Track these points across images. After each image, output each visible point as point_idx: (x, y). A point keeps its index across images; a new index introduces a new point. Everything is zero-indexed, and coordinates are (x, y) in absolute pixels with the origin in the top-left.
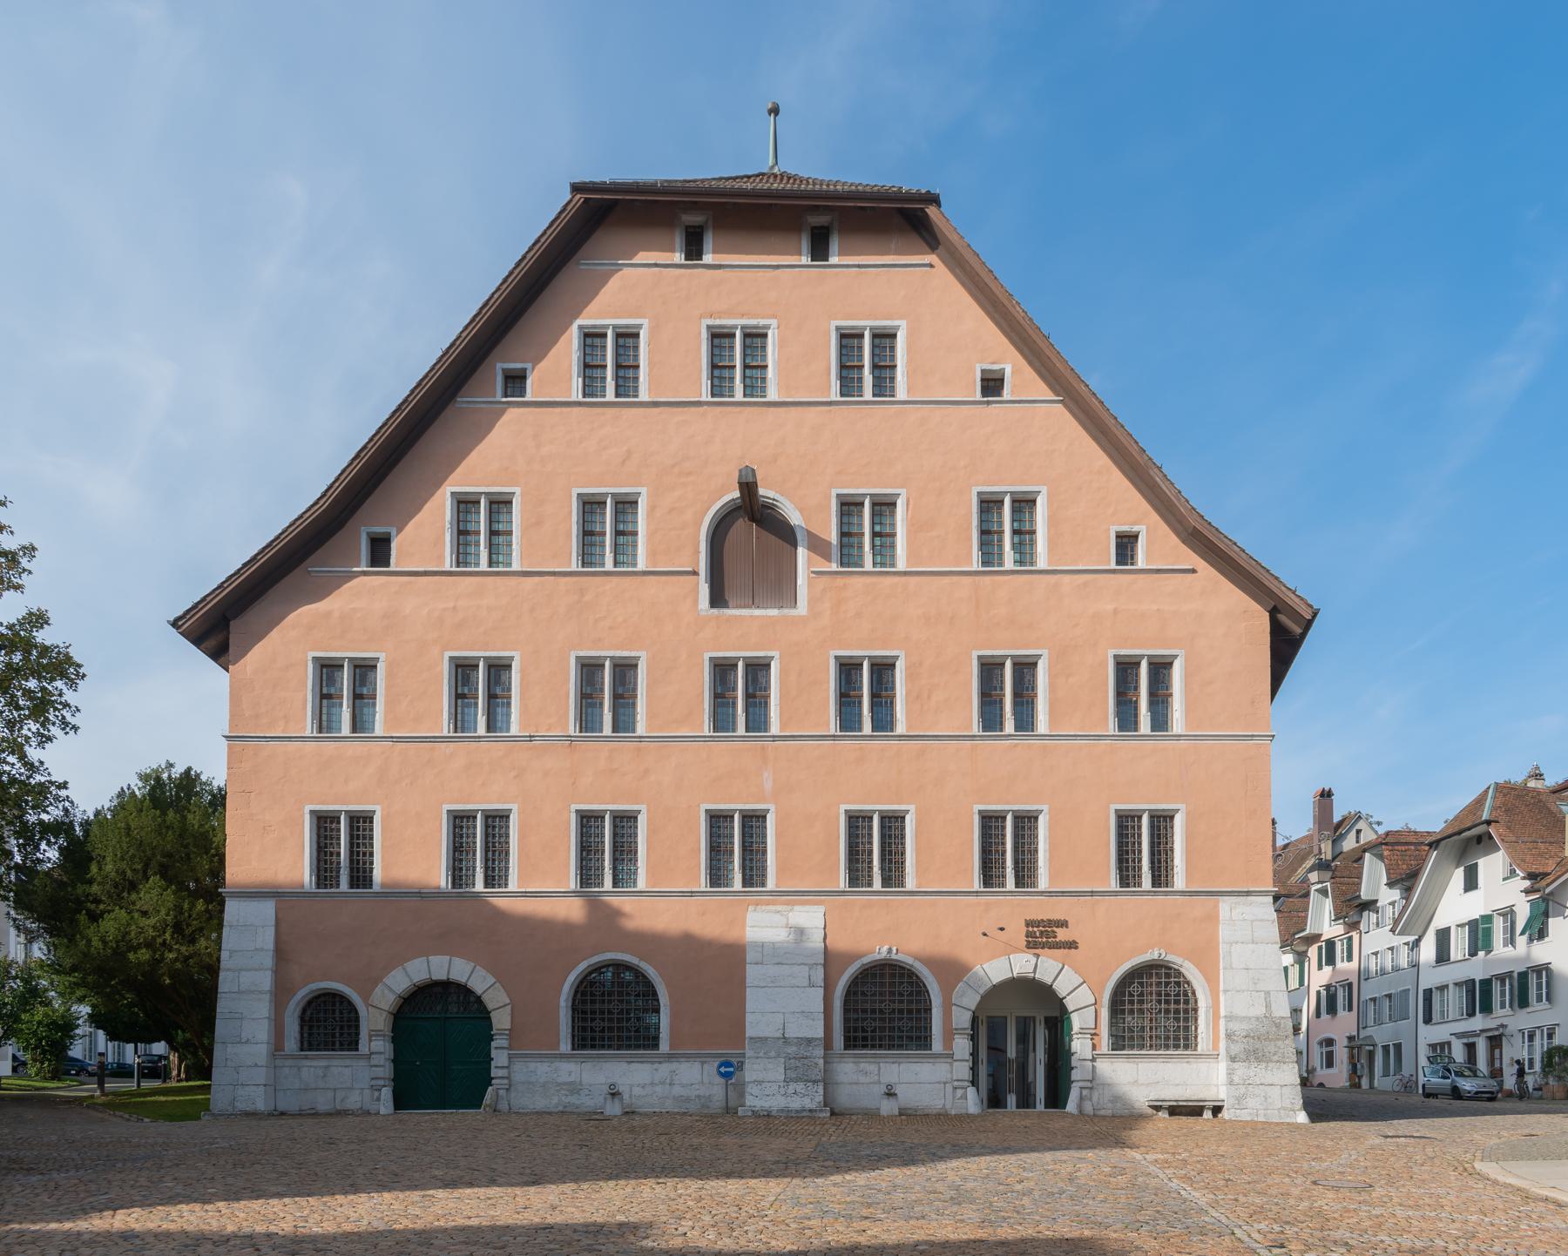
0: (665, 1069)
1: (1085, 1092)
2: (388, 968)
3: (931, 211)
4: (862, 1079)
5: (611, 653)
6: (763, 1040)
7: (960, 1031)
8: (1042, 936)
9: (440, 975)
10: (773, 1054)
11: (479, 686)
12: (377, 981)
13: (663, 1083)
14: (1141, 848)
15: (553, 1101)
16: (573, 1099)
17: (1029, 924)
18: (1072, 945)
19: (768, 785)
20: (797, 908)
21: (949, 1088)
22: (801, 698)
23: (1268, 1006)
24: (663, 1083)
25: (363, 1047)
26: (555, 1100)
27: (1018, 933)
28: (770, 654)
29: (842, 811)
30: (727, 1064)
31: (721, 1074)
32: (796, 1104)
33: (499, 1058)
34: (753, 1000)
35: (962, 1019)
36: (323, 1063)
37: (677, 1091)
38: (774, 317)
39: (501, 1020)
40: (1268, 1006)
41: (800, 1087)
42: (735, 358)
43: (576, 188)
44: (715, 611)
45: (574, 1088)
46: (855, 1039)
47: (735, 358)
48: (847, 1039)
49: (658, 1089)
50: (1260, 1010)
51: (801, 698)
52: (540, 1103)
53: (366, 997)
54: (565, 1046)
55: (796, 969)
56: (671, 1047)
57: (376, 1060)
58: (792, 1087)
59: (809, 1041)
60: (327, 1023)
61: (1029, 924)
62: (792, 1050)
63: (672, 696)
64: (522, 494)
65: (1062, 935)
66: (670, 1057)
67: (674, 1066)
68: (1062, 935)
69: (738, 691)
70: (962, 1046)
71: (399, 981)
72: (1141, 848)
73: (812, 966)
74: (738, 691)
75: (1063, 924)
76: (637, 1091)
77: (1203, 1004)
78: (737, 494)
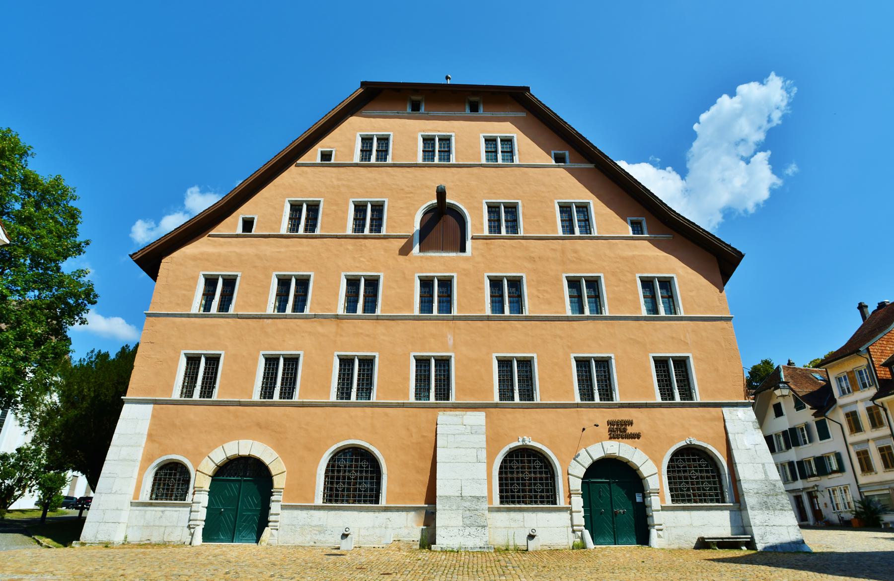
2: (211, 448)
4: (513, 525)
6: (448, 498)
8: (619, 431)
9: (244, 452)
10: (454, 507)
11: (294, 291)
14: (674, 376)
15: (306, 539)
16: (320, 537)
17: (609, 423)
18: (637, 436)
20: (469, 413)
23: (765, 473)
26: (308, 538)
27: (604, 429)
33: (275, 508)
35: (576, 484)
39: (279, 482)
40: (765, 473)
41: (473, 530)
42: (437, 149)
43: (363, 84)
44: (422, 254)
45: (322, 530)
46: (507, 497)
47: (437, 149)
48: (501, 497)
50: (761, 476)
53: (196, 464)
54: (319, 501)
56: (387, 502)
58: (468, 530)
59: (478, 498)
60: (171, 481)
61: (609, 423)
63: (400, 293)
65: (630, 430)
66: (386, 509)
68: (630, 430)
69: (437, 293)
70: (578, 502)
71: (219, 456)
72: (674, 376)
74: (437, 293)
75: (631, 423)
76: (363, 532)
78: (436, 201)
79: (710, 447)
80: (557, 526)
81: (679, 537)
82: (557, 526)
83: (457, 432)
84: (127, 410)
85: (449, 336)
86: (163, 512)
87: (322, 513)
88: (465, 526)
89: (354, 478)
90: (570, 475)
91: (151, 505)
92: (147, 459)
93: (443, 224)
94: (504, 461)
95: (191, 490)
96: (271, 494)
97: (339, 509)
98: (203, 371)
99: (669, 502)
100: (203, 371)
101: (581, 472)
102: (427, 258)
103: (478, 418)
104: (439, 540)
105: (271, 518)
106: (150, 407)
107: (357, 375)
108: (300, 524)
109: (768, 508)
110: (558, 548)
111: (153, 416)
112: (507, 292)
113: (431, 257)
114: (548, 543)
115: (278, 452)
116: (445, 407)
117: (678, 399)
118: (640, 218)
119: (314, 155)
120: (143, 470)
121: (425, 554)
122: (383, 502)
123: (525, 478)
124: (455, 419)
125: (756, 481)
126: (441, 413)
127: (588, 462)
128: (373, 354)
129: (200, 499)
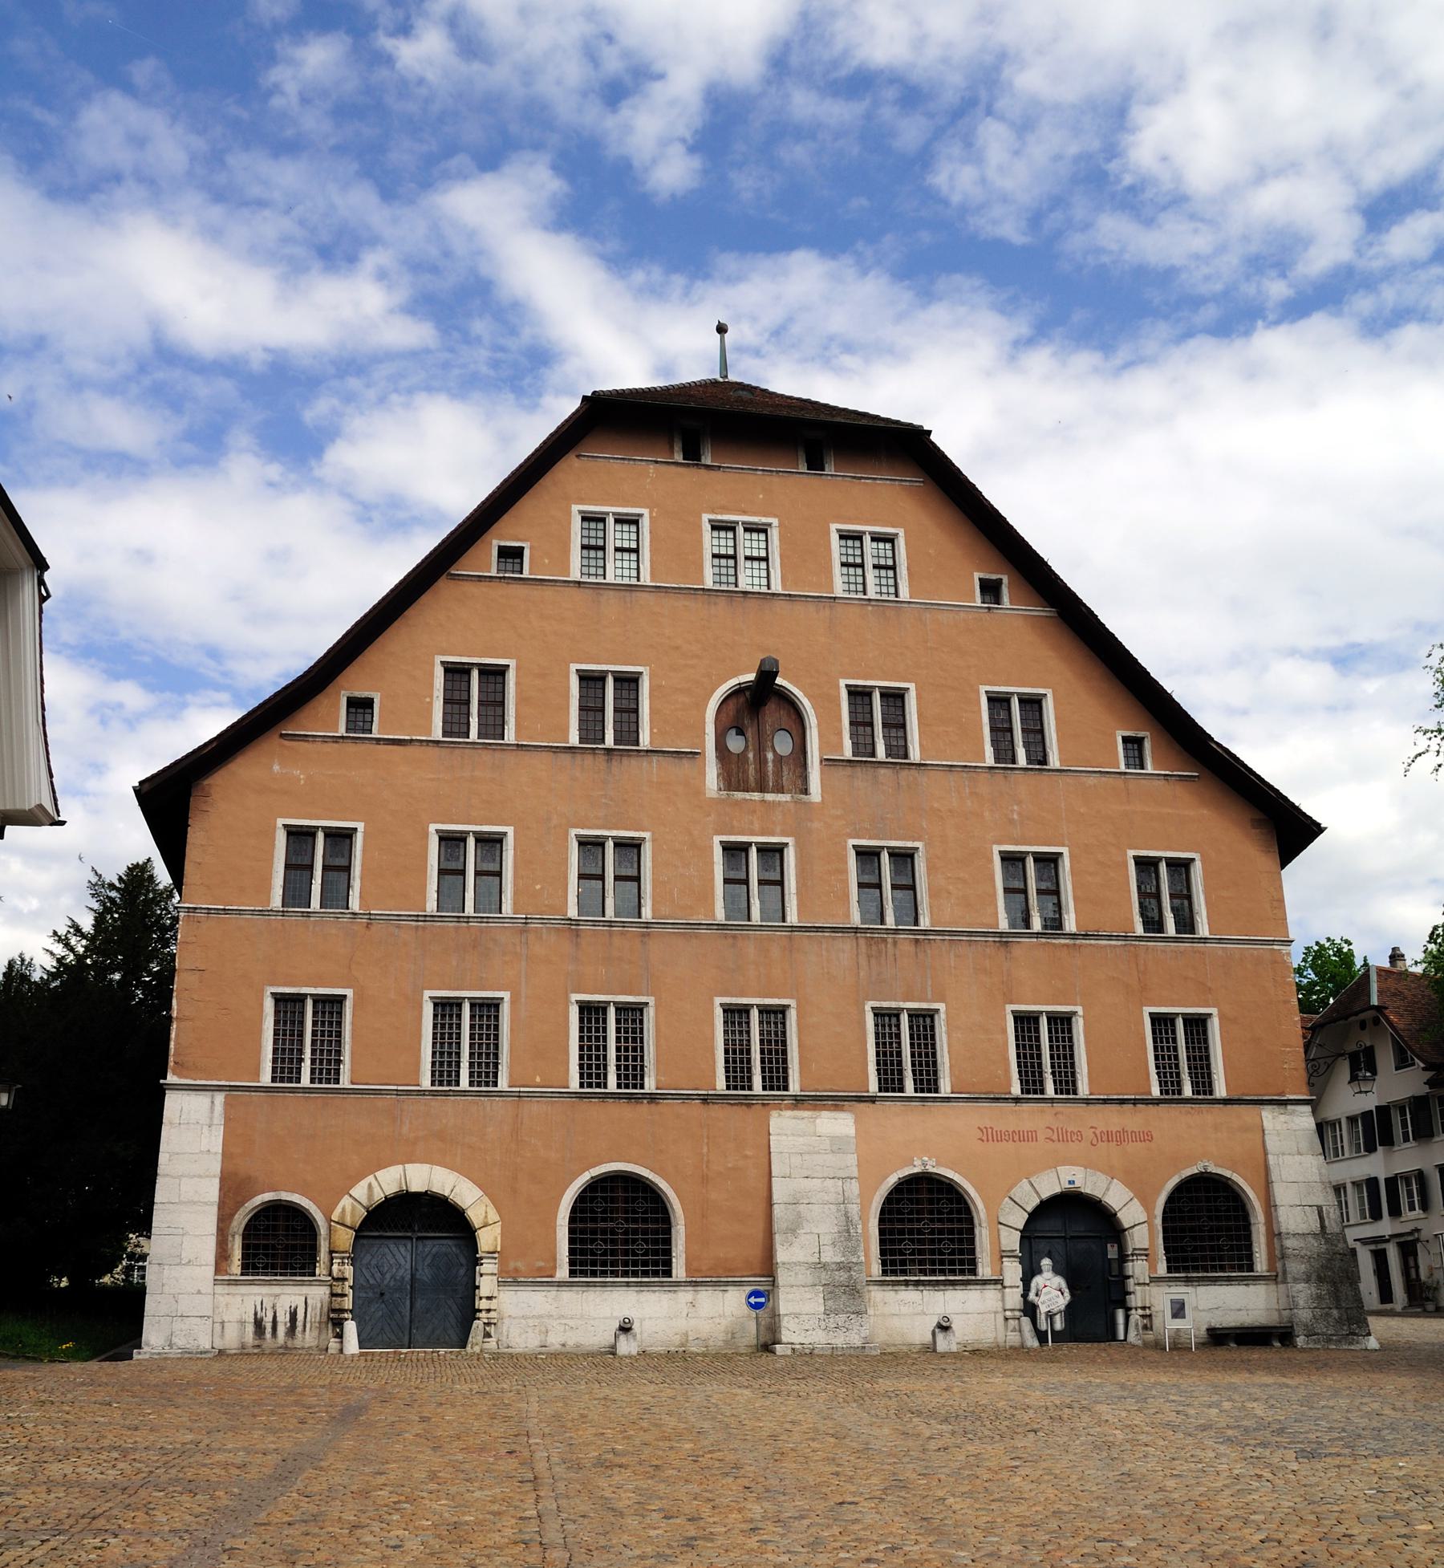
4: (904, 1310)
5: (614, 833)
7: (1011, 1255)
28: (784, 840)
33: (486, 1285)
46: (893, 1263)
54: (563, 1273)
55: (829, 1183)
64: (518, 668)
79: (1236, 1178)
82: (974, 1312)
84: (175, 1105)
87: (568, 1296)
89: (621, 1231)
90: (998, 1229)
94: (888, 1200)
95: (323, 1255)
96: (477, 1262)
97: (604, 1285)
98: (309, 1029)
99: (1162, 1269)
100: (309, 1029)
101: (1019, 1219)
102: (737, 803)
103: (839, 1124)
104: (786, 1336)
106: (220, 1098)
110: (980, 1347)
114: (969, 1338)
116: (779, 1104)
117: (1188, 1091)
119: (485, 558)
121: (765, 1358)
123: (924, 1228)
126: (774, 1114)
127: (1032, 1203)
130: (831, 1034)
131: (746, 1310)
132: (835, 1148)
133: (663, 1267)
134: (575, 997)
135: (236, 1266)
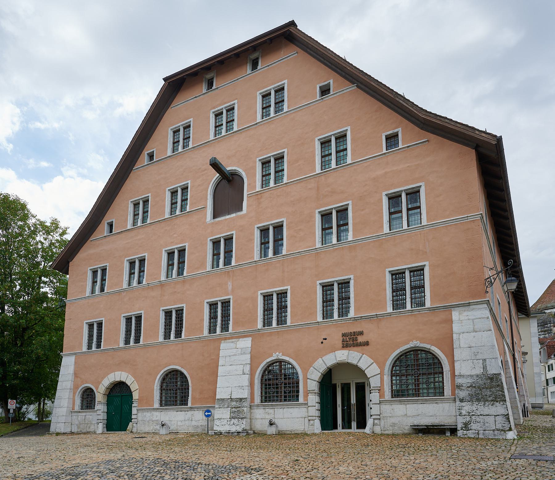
0: (190, 413)
1: (376, 421)
2: (103, 378)
3: (292, 29)
6: (223, 400)
7: (312, 392)
8: (351, 341)
10: (226, 406)
12: (100, 383)
13: (189, 420)
18: (367, 344)
19: (230, 288)
20: (240, 339)
21: (306, 420)
22: (248, 248)
24: (189, 420)
25: (97, 407)
26: (152, 428)
29: (259, 294)
30: (208, 411)
31: (205, 415)
32: (233, 429)
33: (134, 411)
34: (221, 382)
35: (314, 386)
36: (84, 414)
37: (194, 423)
38: (236, 99)
39: (136, 396)
40: (485, 367)
41: (236, 421)
49: (187, 422)
50: (479, 371)
51: (248, 248)
52: (147, 429)
53: (97, 388)
54: (157, 405)
57: (99, 412)
58: (233, 420)
60: (88, 398)
62: (234, 404)
65: (360, 339)
66: (191, 408)
67: (193, 412)
68: (360, 339)
69: (223, 248)
70: (314, 400)
71: (106, 382)
73: (244, 365)
74: (223, 248)
75: (361, 333)
76: (179, 423)
77: (446, 368)
80: (301, 416)
81: (394, 425)
83: (232, 354)
85: (229, 283)
86: (85, 416)
88: (232, 418)
89: (175, 389)
91: (80, 412)
92: (76, 387)
93: (229, 189)
103: (246, 343)
105: (133, 417)
107: (174, 321)
108: (149, 417)
109: (478, 400)
110: (297, 432)
111: (75, 363)
112: (272, 236)
113: (219, 221)
115: (134, 377)
118: (396, 131)
120: (74, 394)
122: (190, 404)
124: (232, 345)
125: (472, 376)
128: (182, 305)
129: (101, 407)
130: (250, 306)
131: (204, 418)
132: (242, 352)
133: (184, 402)
134: (162, 309)
135: (77, 407)
